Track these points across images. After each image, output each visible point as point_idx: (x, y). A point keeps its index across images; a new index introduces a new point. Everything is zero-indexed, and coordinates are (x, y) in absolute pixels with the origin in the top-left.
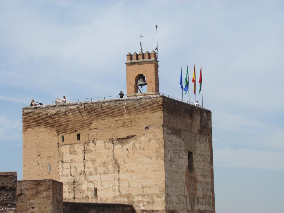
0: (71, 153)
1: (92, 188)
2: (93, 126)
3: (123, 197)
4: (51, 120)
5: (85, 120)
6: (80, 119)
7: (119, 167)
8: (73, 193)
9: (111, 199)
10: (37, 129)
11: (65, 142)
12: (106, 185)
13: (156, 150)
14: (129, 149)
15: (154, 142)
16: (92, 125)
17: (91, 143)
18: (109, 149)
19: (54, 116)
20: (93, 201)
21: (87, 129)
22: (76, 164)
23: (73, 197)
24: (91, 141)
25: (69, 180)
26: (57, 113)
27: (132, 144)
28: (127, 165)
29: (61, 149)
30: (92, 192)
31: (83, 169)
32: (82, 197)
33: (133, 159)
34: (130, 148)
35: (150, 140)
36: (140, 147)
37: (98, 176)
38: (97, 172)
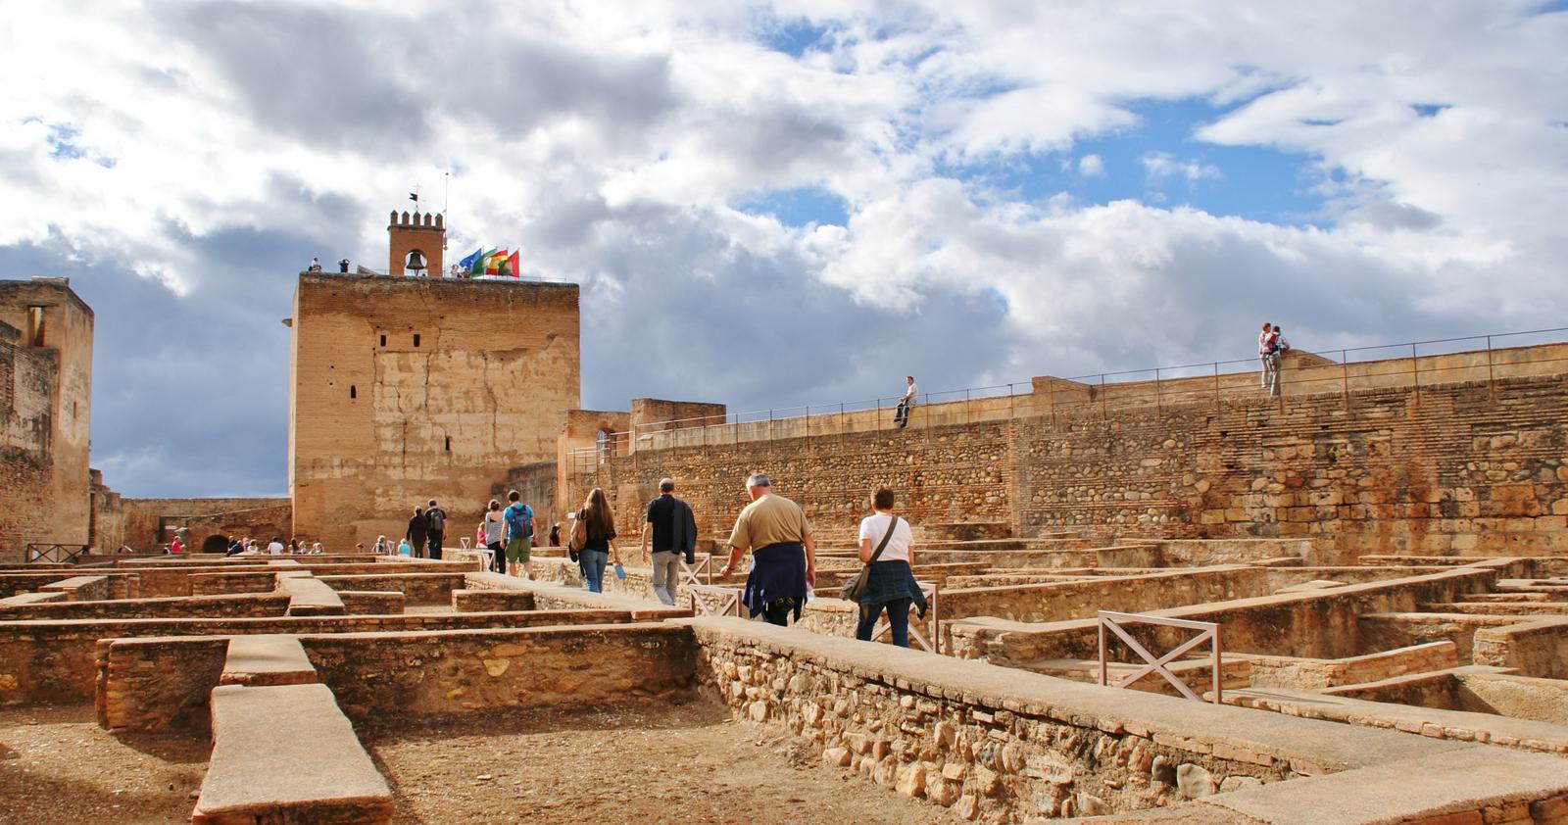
4: (359, 304)
5: (430, 311)
6: (421, 309)
7: (495, 402)
8: (402, 444)
10: (329, 317)
11: (388, 347)
12: (468, 433)
14: (516, 373)
16: (443, 322)
18: (477, 367)
19: (366, 296)
21: (434, 328)
24: (442, 351)
26: (372, 291)
28: (511, 400)
29: (381, 360)
30: (440, 444)
32: (419, 450)
35: (555, 360)
37: (456, 415)
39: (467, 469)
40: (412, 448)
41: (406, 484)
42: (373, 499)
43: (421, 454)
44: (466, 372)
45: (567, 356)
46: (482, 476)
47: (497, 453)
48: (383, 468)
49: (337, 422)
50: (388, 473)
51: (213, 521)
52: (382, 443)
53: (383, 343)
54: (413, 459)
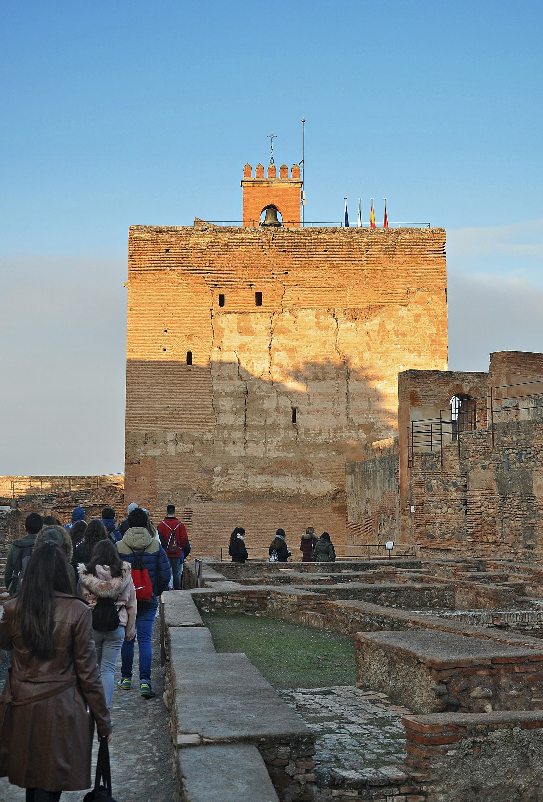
0: (240, 332)
1: (286, 407)
2: (292, 279)
3: (356, 428)
8: (244, 416)
9: (329, 433)
10: (162, 275)
13: (430, 338)
14: (371, 333)
15: (427, 322)
17: (287, 314)
18: (327, 328)
20: (288, 434)
22: (251, 355)
23: (243, 423)
25: (235, 388)
26: (209, 244)
27: (378, 323)
29: (219, 321)
31: (267, 365)
32: (263, 424)
33: (379, 353)
34: (375, 331)
35: (417, 317)
36: (396, 329)
38: (299, 374)
39: (317, 445)
40: (255, 420)
41: (246, 460)
42: (211, 479)
43: (264, 428)
44: (313, 333)
45: (433, 313)
46: (334, 453)
47: (351, 426)
48: (221, 443)
49: (171, 392)
50: (227, 449)
51: (43, 502)
52: (221, 415)
53: (222, 302)
54: (255, 433)
